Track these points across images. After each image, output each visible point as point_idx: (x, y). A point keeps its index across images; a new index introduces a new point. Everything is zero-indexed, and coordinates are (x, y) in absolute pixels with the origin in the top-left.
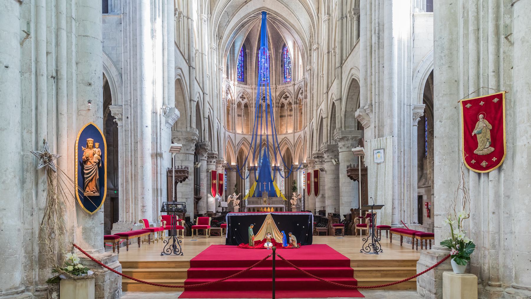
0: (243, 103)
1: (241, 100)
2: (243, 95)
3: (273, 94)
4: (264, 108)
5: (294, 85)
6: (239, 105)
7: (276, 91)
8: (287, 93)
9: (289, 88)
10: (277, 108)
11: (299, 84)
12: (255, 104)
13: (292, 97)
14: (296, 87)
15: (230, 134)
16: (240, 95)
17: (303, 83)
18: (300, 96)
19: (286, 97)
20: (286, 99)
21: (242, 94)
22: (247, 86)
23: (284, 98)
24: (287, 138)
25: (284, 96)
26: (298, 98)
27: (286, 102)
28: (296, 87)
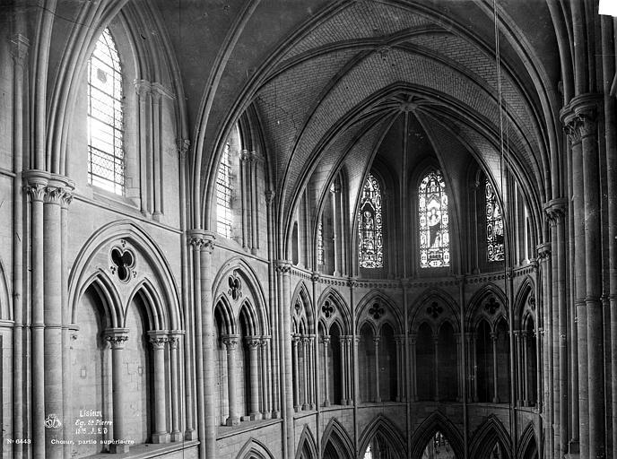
1: (371, 318)
2: (375, 305)
4: (436, 332)
5: (513, 275)
6: (366, 330)
7: (463, 289)
8: (494, 296)
9: (501, 283)
10: (467, 334)
11: (523, 277)
12: (411, 324)
13: (507, 308)
14: (518, 281)
16: (369, 306)
17: (534, 275)
18: (528, 307)
20: (493, 312)
21: (373, 301)
23: (487, 307)
24: (497, 419)
26: (525, 313)
27: (493, 319)
28: (518, 281)
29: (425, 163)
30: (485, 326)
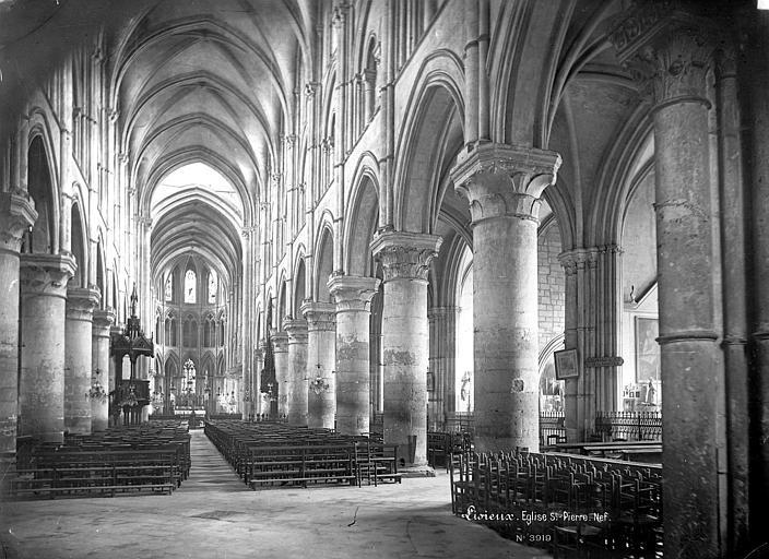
6: (167, 321)
19: (210, 317)
29: (191, 266)
30: (207, 323)
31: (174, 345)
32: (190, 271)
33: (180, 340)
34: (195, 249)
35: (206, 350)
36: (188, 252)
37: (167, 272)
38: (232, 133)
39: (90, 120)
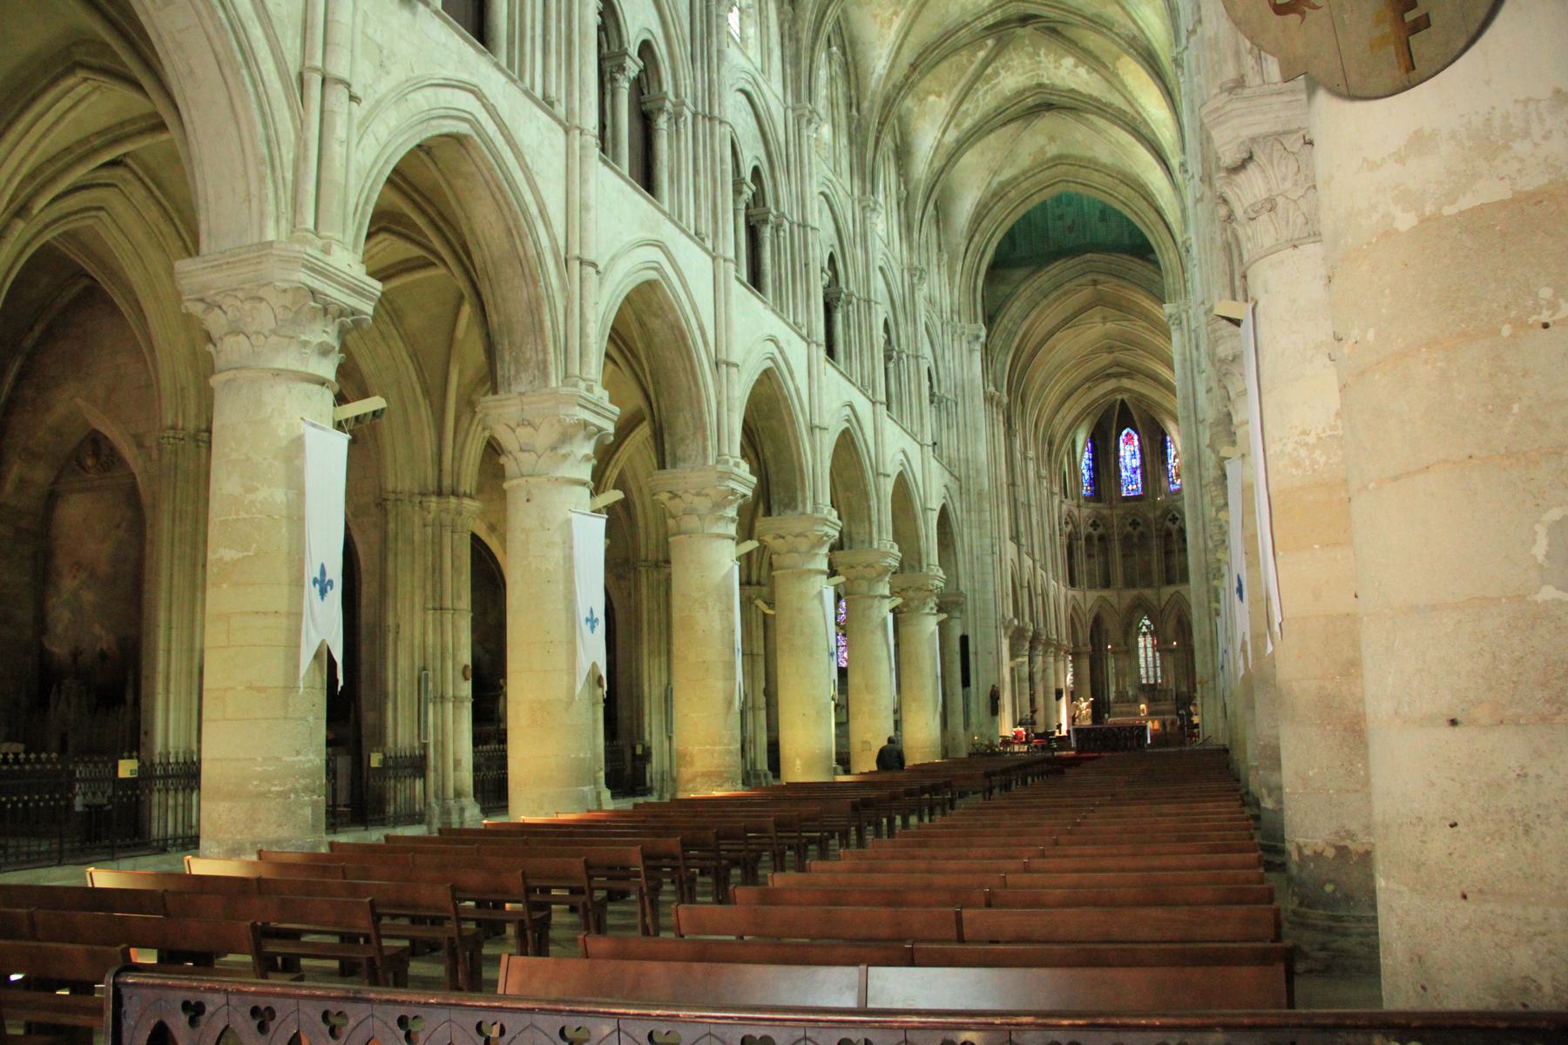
0: (1095, 534)
1: (1091, 530)
3: (1151, 515)
4: (1135, 540)
6: (1089, 538)
15: (1075, 593)
19: (1174, 519)
22: (1100, 505)
25: (1170, 516)
27: (1174, 528)
29: (1125, 419)
30: (1169, 534)
31: (1107, 584)
32: (1125, 432)
33: (1118, 572)
34: (1127, 383)
35: (1171, 589)
36: (1113, 391)
37: (1082, 437)
38: (1103, 109)
39: (711, 119)
